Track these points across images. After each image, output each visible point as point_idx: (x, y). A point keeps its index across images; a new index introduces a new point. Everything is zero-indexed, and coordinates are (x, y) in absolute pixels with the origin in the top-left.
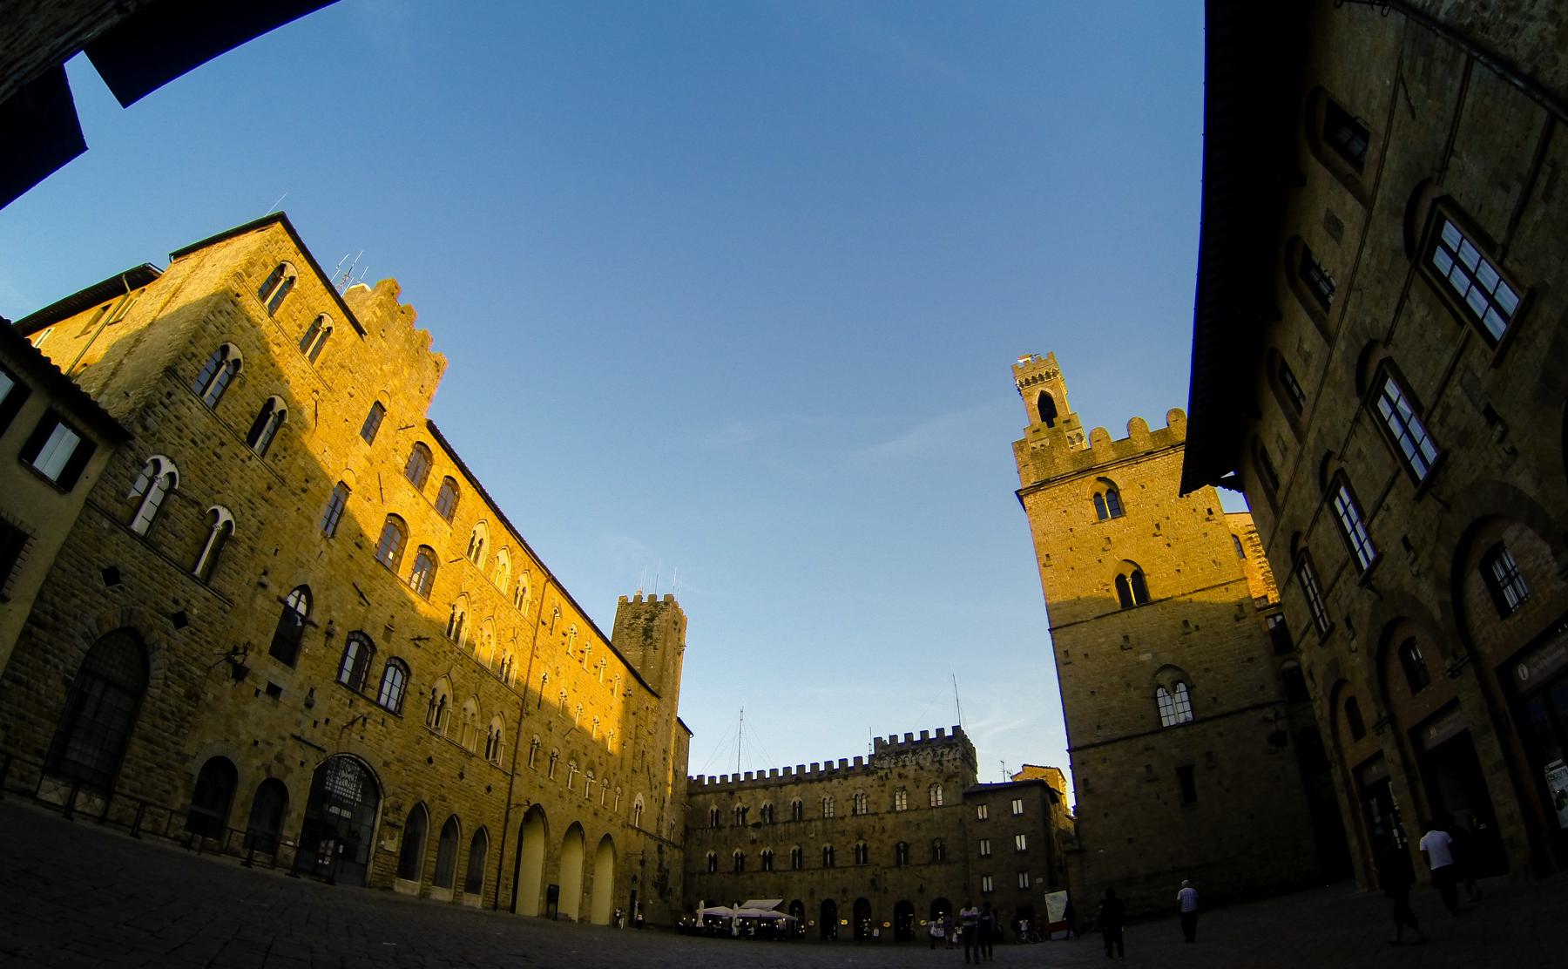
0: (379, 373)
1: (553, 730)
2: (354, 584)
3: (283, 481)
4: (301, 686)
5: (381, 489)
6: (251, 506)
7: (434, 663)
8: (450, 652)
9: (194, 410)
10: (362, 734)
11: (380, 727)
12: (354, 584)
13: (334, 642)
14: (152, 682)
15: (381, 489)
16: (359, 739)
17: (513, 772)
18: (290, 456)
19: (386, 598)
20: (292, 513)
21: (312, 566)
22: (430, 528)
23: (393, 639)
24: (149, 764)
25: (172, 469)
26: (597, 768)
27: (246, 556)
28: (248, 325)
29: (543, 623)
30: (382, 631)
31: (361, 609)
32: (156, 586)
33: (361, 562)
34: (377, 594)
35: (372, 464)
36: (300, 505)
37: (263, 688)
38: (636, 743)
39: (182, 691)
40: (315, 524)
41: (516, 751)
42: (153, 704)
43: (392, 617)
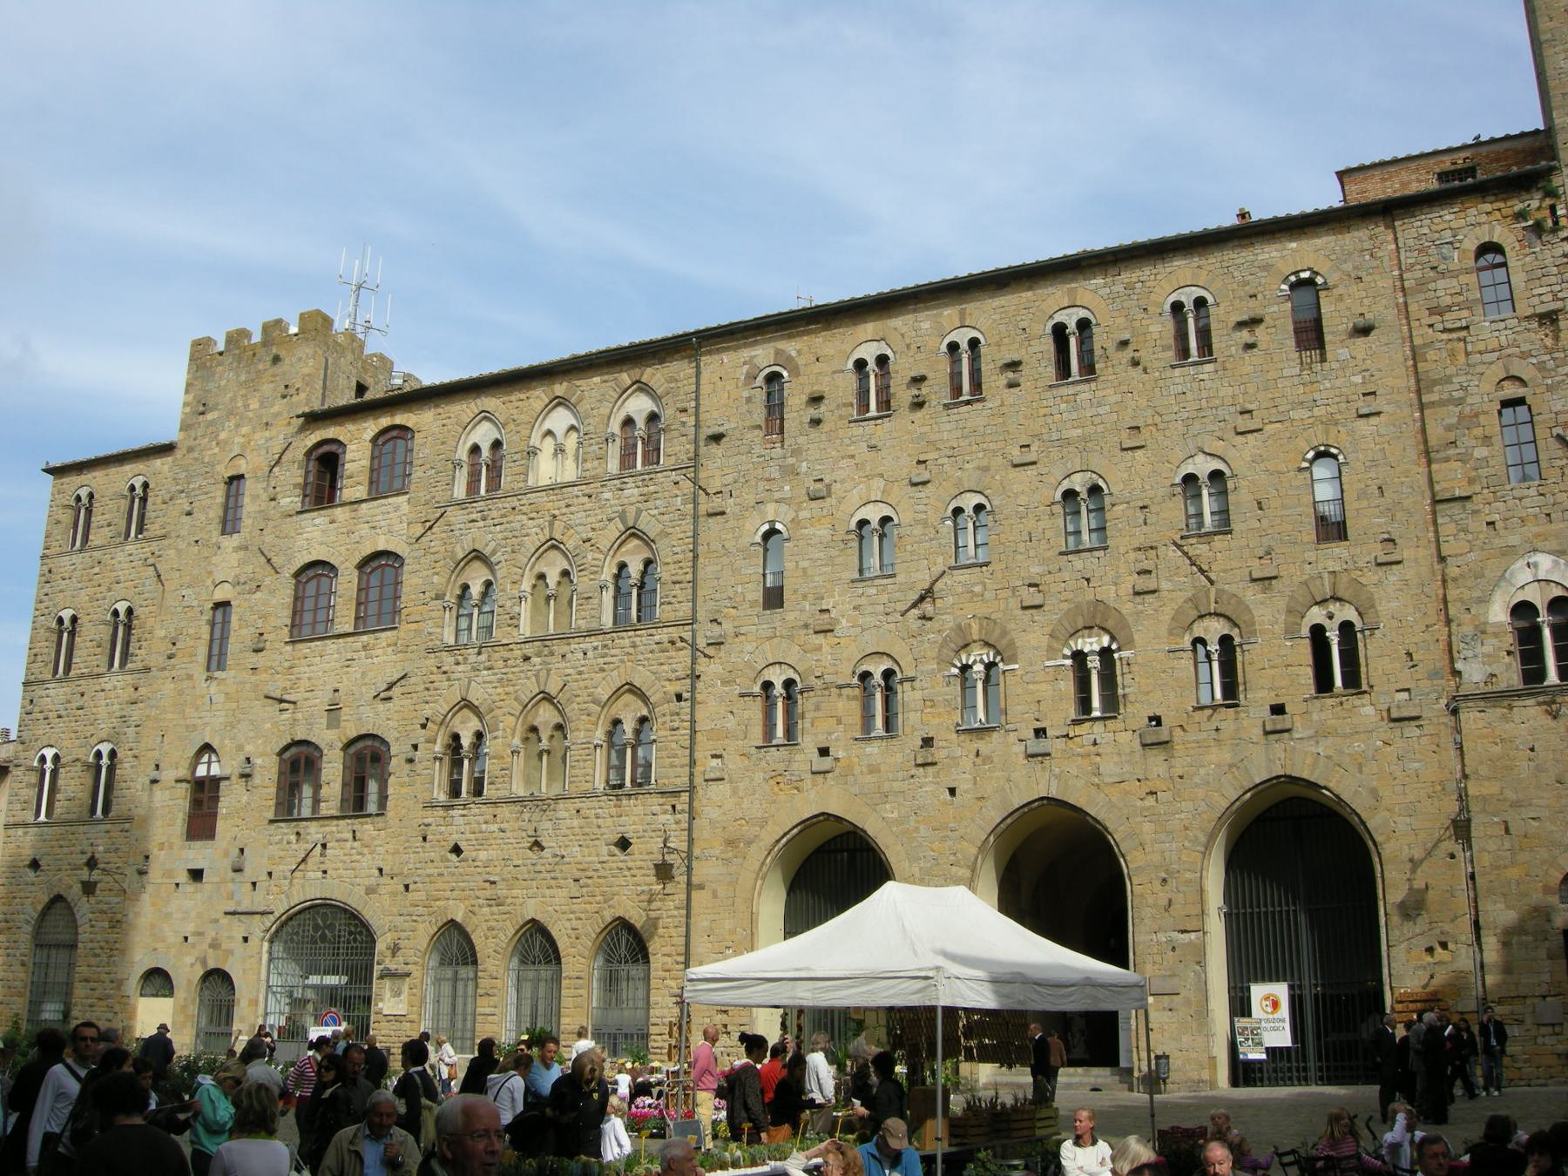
0: (217, 450)
1: (844, 621)
2: (267, 697)
3: (147, 669)
4: (226, 853)
5: (269, 561)
8: (458, 664)
9: (51, 692)
10: (323, 867)
11: (349, 844)
12: (267, 697)
13: (257, 780)
14: (80, 930)
15: (269, 561)
16: (320, 874)
17: (691, 781)
19: (320, 674)
20: (169, 687)
22: (364, 529)
24: (90, 1001)
25: (53, 751)
26: (1127, 609)
27: (132, 767)
28: (67, 581)
29: (717, 438)
30: (324, 721)
31: (286, 715)
32: (66, 850)
33: (269, 664)
34: (304, 684)
35: (246, 548)
36: (174, 673)
37: (183, 877)
38: (1422, 407)
39: (106, 924)
40: (195, 677)
41: (693, 732)
42: (85, 948)
43: (336, 691)
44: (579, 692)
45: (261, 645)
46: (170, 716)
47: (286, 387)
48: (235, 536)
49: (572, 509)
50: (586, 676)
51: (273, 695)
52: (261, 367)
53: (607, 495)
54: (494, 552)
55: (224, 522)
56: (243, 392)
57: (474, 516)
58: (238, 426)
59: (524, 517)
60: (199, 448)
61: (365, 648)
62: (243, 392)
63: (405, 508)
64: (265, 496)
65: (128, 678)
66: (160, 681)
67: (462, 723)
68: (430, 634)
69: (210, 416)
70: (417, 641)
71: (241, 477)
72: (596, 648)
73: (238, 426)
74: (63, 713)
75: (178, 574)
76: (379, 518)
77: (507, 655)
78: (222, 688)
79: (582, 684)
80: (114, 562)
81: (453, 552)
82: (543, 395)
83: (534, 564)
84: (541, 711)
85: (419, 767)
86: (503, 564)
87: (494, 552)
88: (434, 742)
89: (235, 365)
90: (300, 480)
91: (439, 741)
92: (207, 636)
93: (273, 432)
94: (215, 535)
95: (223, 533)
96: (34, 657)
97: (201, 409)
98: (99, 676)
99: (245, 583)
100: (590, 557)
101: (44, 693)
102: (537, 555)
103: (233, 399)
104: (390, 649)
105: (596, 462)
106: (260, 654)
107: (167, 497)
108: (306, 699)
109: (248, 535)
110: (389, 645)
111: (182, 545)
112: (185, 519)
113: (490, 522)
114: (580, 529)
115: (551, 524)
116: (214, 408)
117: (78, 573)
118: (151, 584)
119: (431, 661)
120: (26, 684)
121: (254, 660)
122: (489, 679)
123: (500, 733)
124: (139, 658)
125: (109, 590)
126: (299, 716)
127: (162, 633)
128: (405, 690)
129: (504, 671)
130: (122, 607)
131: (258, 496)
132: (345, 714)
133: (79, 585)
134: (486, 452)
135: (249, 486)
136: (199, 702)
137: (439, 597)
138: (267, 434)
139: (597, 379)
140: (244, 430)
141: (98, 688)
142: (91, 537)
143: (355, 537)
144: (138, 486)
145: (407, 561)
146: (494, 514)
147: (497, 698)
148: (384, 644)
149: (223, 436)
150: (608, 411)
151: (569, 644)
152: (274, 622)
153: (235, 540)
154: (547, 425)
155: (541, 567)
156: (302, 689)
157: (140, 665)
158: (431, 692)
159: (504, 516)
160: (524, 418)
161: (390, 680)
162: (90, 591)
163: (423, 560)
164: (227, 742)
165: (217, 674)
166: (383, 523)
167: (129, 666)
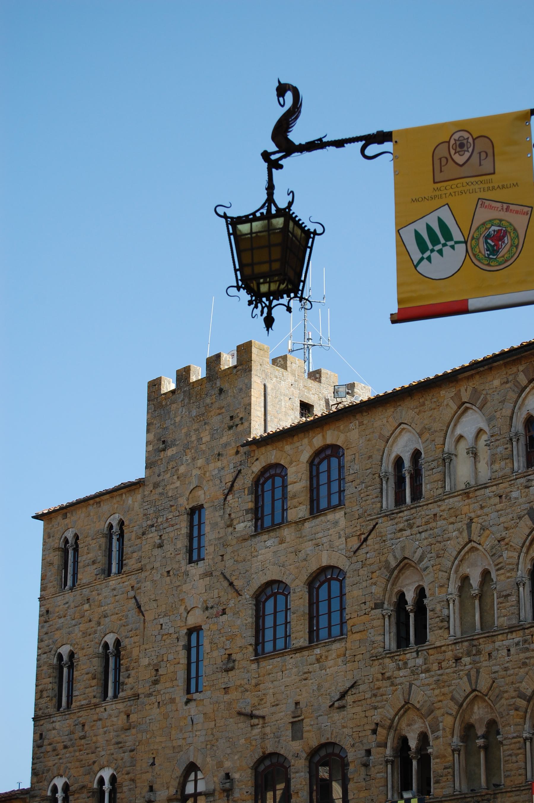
0: (178, 484)
2: (240, 714)
3: (137, 696)
6: (120, 745)
7: (376, 708)
8: (399, 669)
12: (240, 714)
15: (231, 584)
18: (133, 669)
19: (283, 688)
21: (189, 740)
23: (306, 728)
28: (62, 620)
30: (289, 733)
31: (256, 731)
34: (270, 699)
40: (177, 700)
44: (506, 688)
45: (231, 665)
46: (158, 739)
47: (232, 418)
48: (201, 563)
49: (486, 510)
50: (511, 672)
51: (243, 711)
52: (208, 401)
53: (514, 495)
54: (421, 559)
55: (190, 551)
56: (195, 426)
57: (401, 526)
58: (194, 459)
59: (445, 522)
60: (163, 484)
61: (318, 661)
62: (195, 426)
63: (343, 523)
64: (222, 524)
65: (121, 706)
66: (148, 707)
67: (409, 725)
68: (373, 642)
69: (170, 452)
70: (363, 650)
71: (201, 507)
72: (517, 644)
73: (194, 459)
74: (69, 744)
75: (154, 604)
76: (320, 535)
77: (440, 657)
78: (200, 708)
79: (508, 680)
80: (100, 597)
81: (387, 561)
82: (451, 403)
83: (459, 566)
84: (476, 708)
85: (373, 771)
86: (431, 569)
87: (421, 559)
88: (385, 746)
89: (186, 401)
90: (251, 505)
91: (389, 745)
92: (184, 661)
93: (224, 461)
94: (184, 566)
95: (191, 561)
96: (40, 694)
97: (162, 446)
98: (96, 706)
99: (212, 607)
100: (505, 555)
101: (50, 726)
102: (459, 558)
103: (188, 435)
104: (340, 660)
105: (503, 463)
106: (231, 673)
107: (140, 532)
108: (273, 714)
109: (211, 562)
110: (338, 656)
111: (157, 577)
112: (156, 551)
113: (415, 530)
114: (494, 529)
115: (469, 526)
116: (173, 444)
117: (71, 611)
118: (133, 614)
119: (376, 669)
120: (34, 719)
121: (226, 680)
122: (426, 681)
123: (440, 733)
124: (129, 686)
125: (99, 624)
126: (268, 730)
127: (145, 661)
128: (355, 697)
129: (440, 672)
130: (110, 639)
131: (216, 524)
132: (307, 725)
133: (73, 622)
134: (407, 464)
135: (208, 515)
136: (182, 724)
137: (378, 606)
138: (219, 464)
139: (496, 383)
140: (200, 462)
141: (95, 717)
142: (79, 576)
143: (302, 555)
144: (115, 524)
145: (348, 575)
146: (418, 522)
147: (435, 699)
148: (334, 656)
149: (182, 469)
150: (508, 413)
151: (494, 642)
152: (240, 642)
153: (200, 568)
154: (459, 431)
155: (466, 570)
156: (268, 704)
157: (129, 693)
158: (378, 698)
159: (427, 523)
160: (436, 426)
161: (342, 689)
162: (82, 627)
163: (361, 572)
164: (208, 759)
165: (196, 696)
166: (325, 540)
167: (121, 694)
